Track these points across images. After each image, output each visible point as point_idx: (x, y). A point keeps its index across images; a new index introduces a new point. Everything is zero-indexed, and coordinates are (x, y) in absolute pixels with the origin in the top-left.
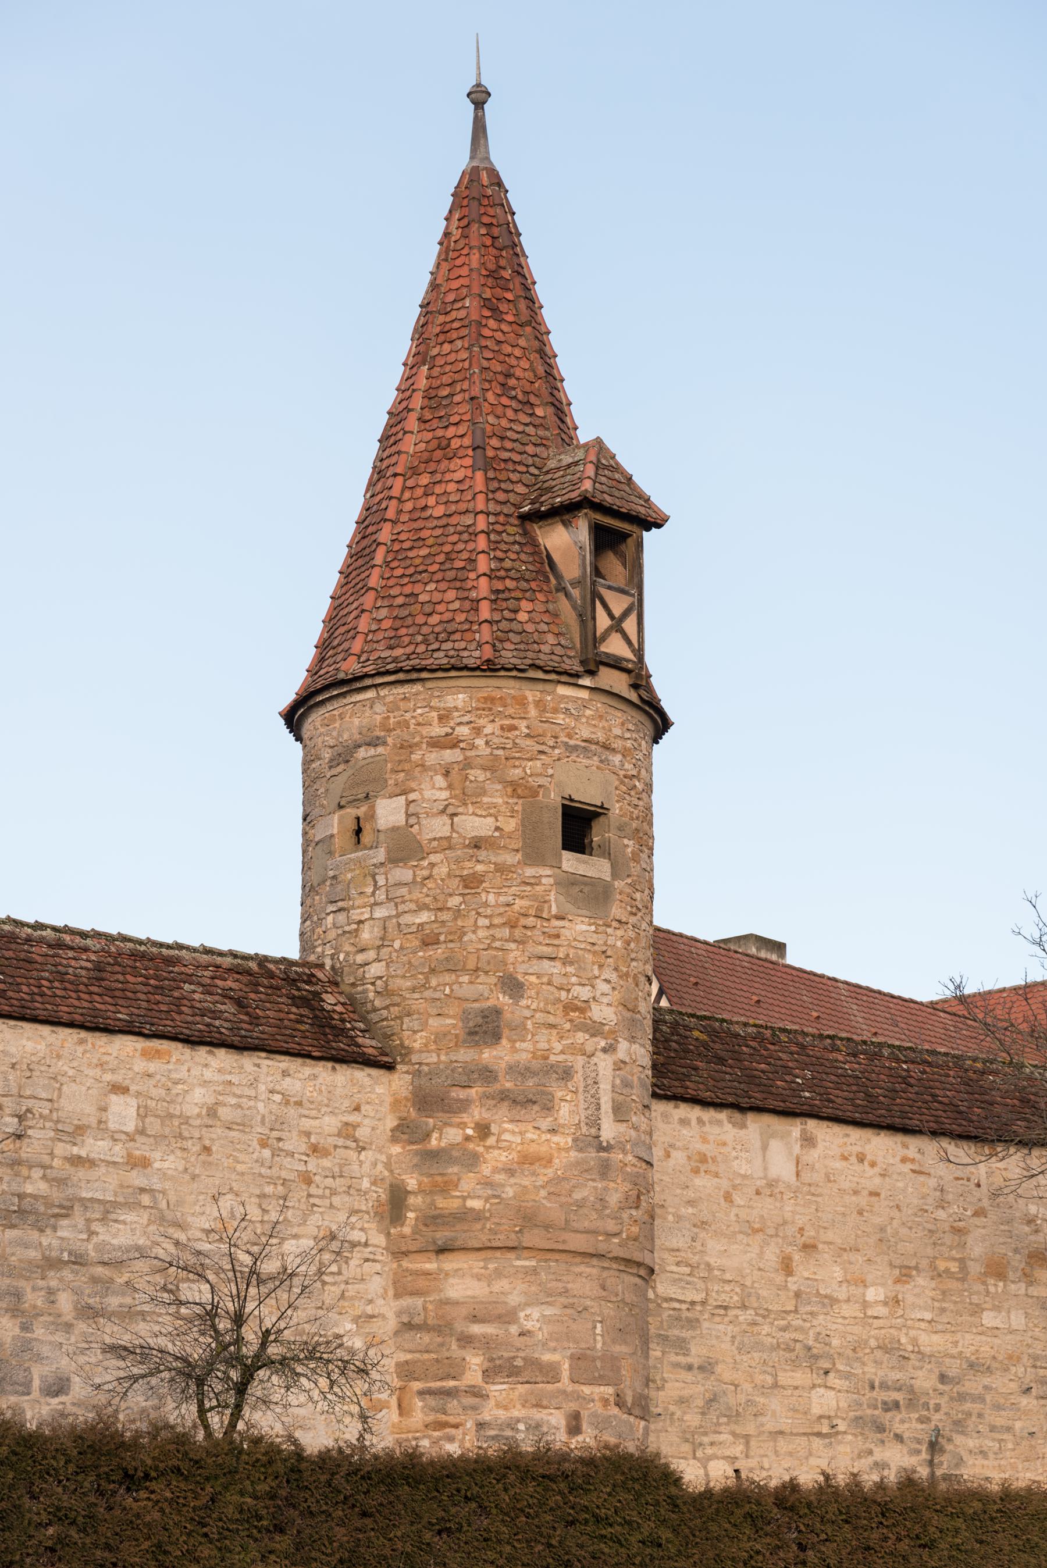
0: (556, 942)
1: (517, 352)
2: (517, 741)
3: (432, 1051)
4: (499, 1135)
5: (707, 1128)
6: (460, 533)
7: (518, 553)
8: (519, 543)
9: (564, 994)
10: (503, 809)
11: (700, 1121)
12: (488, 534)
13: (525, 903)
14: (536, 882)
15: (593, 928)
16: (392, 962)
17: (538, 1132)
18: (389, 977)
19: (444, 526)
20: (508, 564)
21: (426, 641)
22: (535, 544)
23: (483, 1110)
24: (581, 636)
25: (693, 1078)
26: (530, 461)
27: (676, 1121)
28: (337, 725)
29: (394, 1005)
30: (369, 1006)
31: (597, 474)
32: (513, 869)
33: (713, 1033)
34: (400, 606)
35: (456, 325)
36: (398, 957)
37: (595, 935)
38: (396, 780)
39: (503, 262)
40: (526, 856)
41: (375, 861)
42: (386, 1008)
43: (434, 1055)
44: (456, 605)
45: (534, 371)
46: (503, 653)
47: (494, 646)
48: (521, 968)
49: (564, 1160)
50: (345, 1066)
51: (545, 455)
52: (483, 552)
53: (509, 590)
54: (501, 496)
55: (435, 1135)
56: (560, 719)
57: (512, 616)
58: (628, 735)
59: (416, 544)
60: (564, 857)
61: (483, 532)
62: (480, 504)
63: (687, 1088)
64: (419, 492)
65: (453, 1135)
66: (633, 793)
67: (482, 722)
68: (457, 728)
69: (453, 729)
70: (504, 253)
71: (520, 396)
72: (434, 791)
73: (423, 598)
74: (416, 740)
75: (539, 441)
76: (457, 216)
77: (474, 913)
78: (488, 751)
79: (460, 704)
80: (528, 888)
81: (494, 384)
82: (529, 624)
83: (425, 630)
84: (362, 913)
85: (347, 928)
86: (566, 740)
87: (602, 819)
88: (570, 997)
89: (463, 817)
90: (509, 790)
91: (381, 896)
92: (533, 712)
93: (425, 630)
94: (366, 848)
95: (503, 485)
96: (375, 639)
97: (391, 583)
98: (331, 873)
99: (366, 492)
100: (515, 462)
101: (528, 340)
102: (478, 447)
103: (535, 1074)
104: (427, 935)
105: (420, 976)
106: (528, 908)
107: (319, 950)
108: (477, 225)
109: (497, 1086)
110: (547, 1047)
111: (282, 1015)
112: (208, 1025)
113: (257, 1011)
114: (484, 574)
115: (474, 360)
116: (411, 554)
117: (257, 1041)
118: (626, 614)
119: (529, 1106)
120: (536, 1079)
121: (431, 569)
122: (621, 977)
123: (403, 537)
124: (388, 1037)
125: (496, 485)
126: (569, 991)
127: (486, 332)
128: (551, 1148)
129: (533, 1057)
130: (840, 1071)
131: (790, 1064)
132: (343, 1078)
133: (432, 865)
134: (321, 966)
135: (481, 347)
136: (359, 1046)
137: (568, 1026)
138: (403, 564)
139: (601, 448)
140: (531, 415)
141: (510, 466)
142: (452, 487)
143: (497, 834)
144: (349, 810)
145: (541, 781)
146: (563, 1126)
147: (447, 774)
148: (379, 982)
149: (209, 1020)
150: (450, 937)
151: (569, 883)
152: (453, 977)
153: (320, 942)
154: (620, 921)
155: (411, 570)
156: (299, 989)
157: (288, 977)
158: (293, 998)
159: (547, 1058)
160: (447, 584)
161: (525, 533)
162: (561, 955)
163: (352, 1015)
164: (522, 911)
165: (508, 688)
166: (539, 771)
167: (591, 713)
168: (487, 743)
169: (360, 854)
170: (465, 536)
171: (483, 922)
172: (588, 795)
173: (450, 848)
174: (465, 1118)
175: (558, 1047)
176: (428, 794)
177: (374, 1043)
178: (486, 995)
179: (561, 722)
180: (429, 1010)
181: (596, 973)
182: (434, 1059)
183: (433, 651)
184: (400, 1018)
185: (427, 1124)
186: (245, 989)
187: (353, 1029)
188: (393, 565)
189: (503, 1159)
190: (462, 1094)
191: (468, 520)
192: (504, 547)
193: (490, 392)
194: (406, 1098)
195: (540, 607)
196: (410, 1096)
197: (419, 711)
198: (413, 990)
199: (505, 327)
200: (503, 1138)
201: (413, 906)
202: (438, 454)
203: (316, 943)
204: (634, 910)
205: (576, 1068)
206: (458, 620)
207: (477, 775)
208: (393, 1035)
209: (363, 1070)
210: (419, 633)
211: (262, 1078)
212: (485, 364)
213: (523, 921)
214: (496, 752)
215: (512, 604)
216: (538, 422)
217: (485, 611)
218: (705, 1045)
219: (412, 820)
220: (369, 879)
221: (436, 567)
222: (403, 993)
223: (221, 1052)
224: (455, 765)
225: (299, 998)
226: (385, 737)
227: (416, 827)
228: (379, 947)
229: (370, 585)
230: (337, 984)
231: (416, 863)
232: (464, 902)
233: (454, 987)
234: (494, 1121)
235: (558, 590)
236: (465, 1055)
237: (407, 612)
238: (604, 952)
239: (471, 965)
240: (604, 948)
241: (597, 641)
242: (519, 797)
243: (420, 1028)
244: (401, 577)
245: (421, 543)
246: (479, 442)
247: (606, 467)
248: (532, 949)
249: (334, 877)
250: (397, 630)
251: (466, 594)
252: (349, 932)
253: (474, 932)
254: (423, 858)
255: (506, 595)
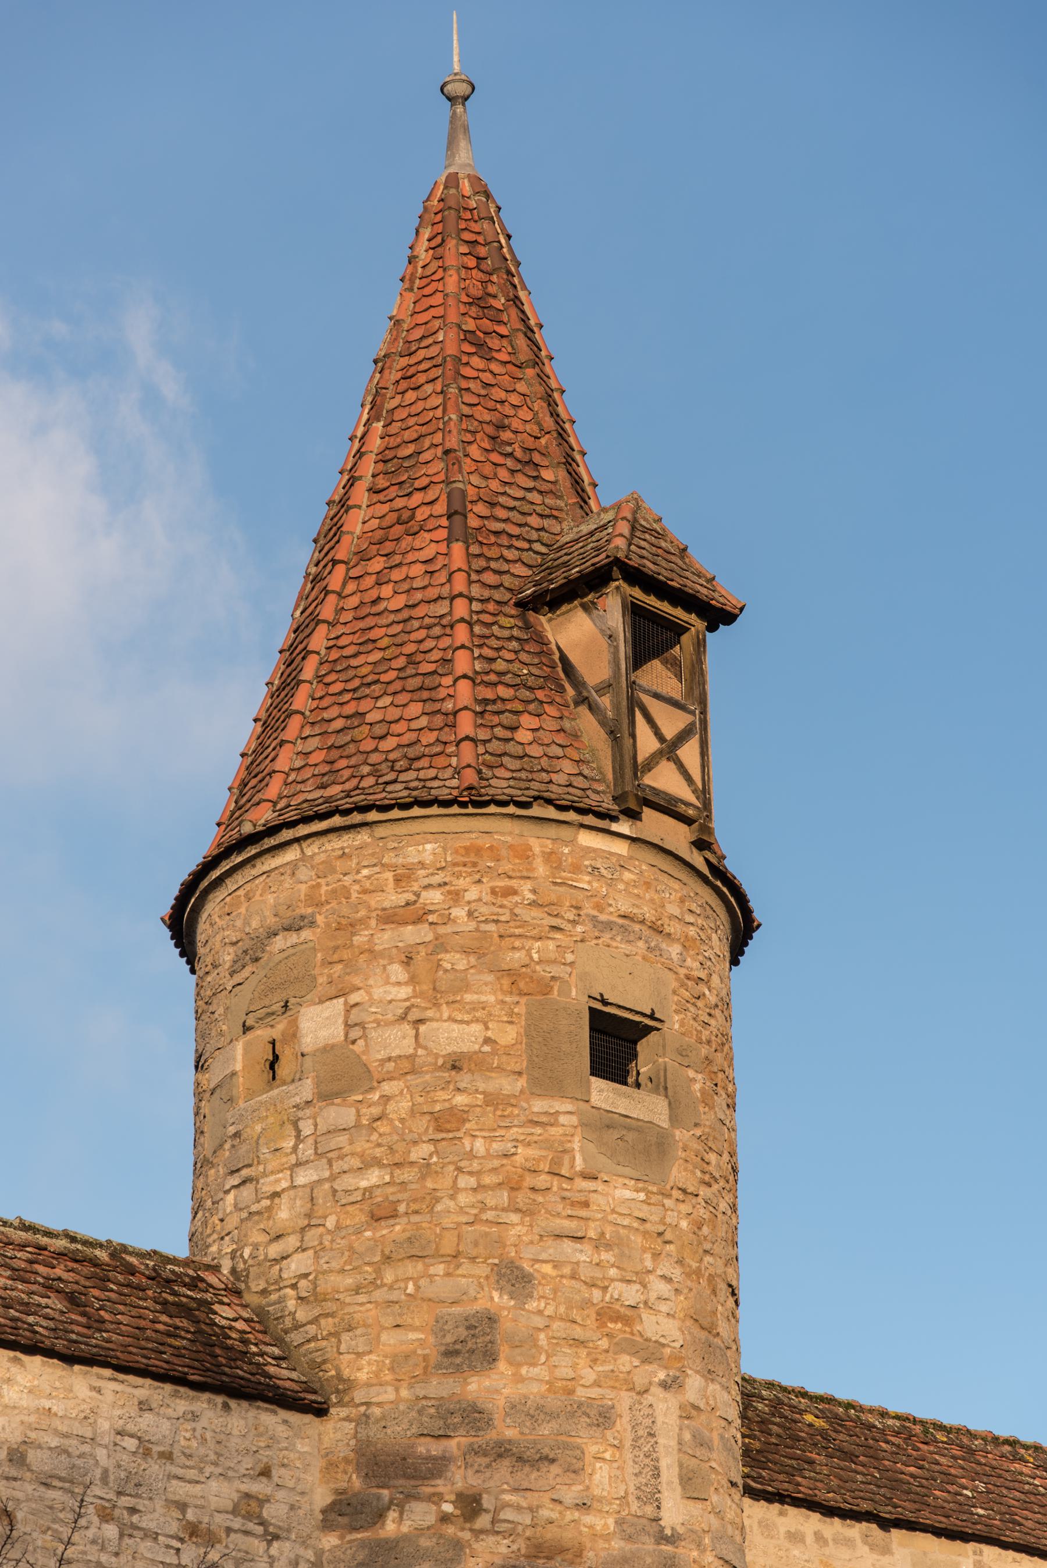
0: (583, 1213)
1: (514, 399)
2: (517, 911)
3: (387, 1383)
4: (496, 1511)
5: (831, 1549)
6: (429, 627)
7: (516, 652)
8: (518, 639)
9: (597, 1294)
10: (496, 1011)
11: (819, 1537)
12: (470, 624)
13: (533, 1152)
14: (551, 1119)
15: (642, 1196)
16: (323, 1249)
17: (559, 1508)
18: (318, 1272)
19: (405, 621)
20: (500, 666)
21: (376, 773)
22: (541, 640)
23: (470, 1472)
24: (613, 761)
25: (807, 1474)
26: (534, 535)
27: (782, 1536)
28: (243, 910)
29: (327, 1315)
30: (288, 1322)
31: (632, 535)
32: (513, 1101)
33: (836, 1421)
34: (338, 732)
35: (423, 366)
36: (332, 1241)
37: (645, 1207)
38: (330, 976)
39: (492, 289)
40: (534, 1082)
41: (297, 1100)
42: (315, 1321)
43: (390, 1389)
44: (424, 721)
45: (539, 424)
46: (493, 782)
47: (479, 772)
48: (528, 1253)
49: (603, 1554)
50: (245, 1404)
51: (557, 529)
52: (463, 647)
53: (503, 700)
54: (490, 578)
55: (392, 1515)
56: (584, 881)
57: (508, 734)
58: (690, 918)
59: (362, 649)
60: (594, 1086)
61: (462, 620)
62: (460, 584)
63: (798, 1484)
64: (369, 581)
65: (421, 1514)
66: (700, 1003)
67: (462, 883)
68: (424, 894)
69: (418, 896)
70: (494, 278)
71: (519, 453)
72: (389, 988)
73: (370, 718)
74: (362, 913)
75: (547, 512)
76: (426, 236)
77: (451, 1168)
78: (472, 925)
79: (428, 858)
80: (538, 1130)
81: (479, 436)
82: (535, 745)
83: (374, 758)
84: (278, 1181)
85: (254, 1208)
86: (595, 913)
87: (653, 1037)
88: (607, 1298)
89: (435, 1025)
90: (506, 982)
91: (306, 1151)
92: (541, 870)
93: (374, 758)
94: (284, 1083)
95: (493, 565)
96: (299, 779)
97: (325, 703)
98: (232, 1130)
99: (295, 609)
100: (511, 536)
101: (529, 385)
102: (456, 513)
103: (552, 1416)
104: (378, 1205)
105: (368, 1269)
106: (538, 1160)
107: (214, 1249)
108: (454, 242)
109: (492, 1435)
110: (571, 1375)
111: (142, 1323)
112: (13, 1319)
113: (102, 1313)
114: (465, 676)
115: (450, 404)
116: (354, 662)
117: (95, 1350)
118: (683, 737)
119: (544, 1466)
120: (554, 1425)
121: (384, 678)
122: (688, 1275)
123: (342, 642)
124: (319, 1366)
125: (483, 563)
126: (605, 1289)
127: (467, 371)
128: (580, 1533)
129: (549, 1390)
130: (1027, 1487)
131: (953, 1471)
132: (242, 1422)
133: (386, 1099)
134: (215, 1269)
135: (461, 390)
136: (270, 1377)
137: (604, 1343)
138: (343, 676)
139: (638, 507)
140: (535, 478)
141: (504, 540)
142: (417, 570)
143: (487, 1048)
144: (259, 1032)
145: (556, 970)
146: (600, 1500)
147: (408, 961)
148: (303, 1284)
149: (17, 1314)
150: (414, 1207)
151: (603, 1125)
152: (420, 1266)
153: (215, 1236)
154: (684, 1191)
155: (356, 682)
156: (175, 1294)
157: (159, 1275)
158: (165, 1303)
159: (571, 1392)
160: (409, 696)
161: (527, 626)
162: (592, 1234)
163: (260, 1336)
164: (528, 1165)
165: (502, 834)
166: (552, 956)
167: (632, 877)
168: (470, 914)
169: (276, 1091)
170: (437, 631)
171: (464, 1181)
172: (631, 996)
173: (413, 1072)
174: (440, 1486)
175: (589, 1375)
176: (378, 993)
177: (294, 1375)
178: (472, 1293)
179: (586, 886)
180: (382, 1320)
181: (649, 1264)
182: (389, 1395)
183: (387, 783)
184: (336, 1334)
185: (379, 1498)
186: (83, 1281)
187: (262, 1354)
188: (328, 680)
189: (504, 1550)
190: (435, 1448)
191: (442, 608)
192: (494, 643)
193: (474, 446)
194: (346, 1460)
195: (551, 725)
196: (352, 1455)
197: (365, 872)
198: (357, 1290)
199: (495, 367)
200: (502, 1516)
201: (356, 1163)
202: (398, 530)
203: (210, 1240)
204: (707, 1178)
205: (619, 1409)
206: (424, 742)
207: (454, 960)
208: (324, 1362)
209: (275, 1413)
210: (365, 763)
211: (104, 1409)
212: (466, 410)
213: (529, 1181)
214: (484, 927)
215: (507, 719)
216: (545, 487)
217: (466, 725)
218: (822, 1433)
219: (355, 1033)
220: (290, 1130)
221: (392, 675)
222: (341, 1296)
223: (36, 1362)
224: (421, 948)
225: (174, 1304)
226: (313, 915)
227: (361, 1043)
228: (303, 1230)
229: (293, 707)
230: (238, 1293)
231: (360, 1098)
232: (437, 1152)
233: (422, 1282)
234: (487, 1490)
235: (577, 704)
236: (440, 1387)
237: (348, 738)
238: (660, 1234)
239: (448, 1246)
240: (661, 1229)
241: (639, 769)
242: (521, 994)
243: (367, 1349)
244: (340, 693)
245: (370, 646)
246: (457, 506)
247: (646, 530)
248: (543, 1222)
249: (237, 1135)
250: (332, 763)
251: (437, 706)
252: (258, 1213)
253: (452, 1197)
254: (372, 1089)
255: (499, 706)
